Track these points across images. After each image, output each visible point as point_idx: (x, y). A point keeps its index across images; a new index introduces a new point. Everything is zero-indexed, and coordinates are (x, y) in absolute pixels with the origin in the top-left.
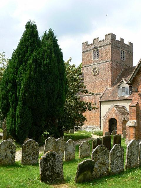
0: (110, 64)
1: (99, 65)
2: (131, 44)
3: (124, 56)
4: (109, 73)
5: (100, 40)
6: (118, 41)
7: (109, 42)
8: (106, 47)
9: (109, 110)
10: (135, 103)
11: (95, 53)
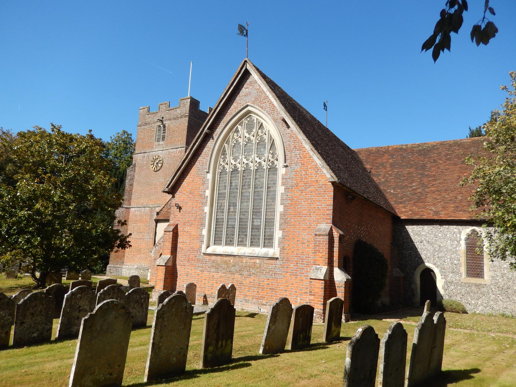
1: (163, 152)
7: (186, 113)
8: (180, 120)
11: (160, 130)
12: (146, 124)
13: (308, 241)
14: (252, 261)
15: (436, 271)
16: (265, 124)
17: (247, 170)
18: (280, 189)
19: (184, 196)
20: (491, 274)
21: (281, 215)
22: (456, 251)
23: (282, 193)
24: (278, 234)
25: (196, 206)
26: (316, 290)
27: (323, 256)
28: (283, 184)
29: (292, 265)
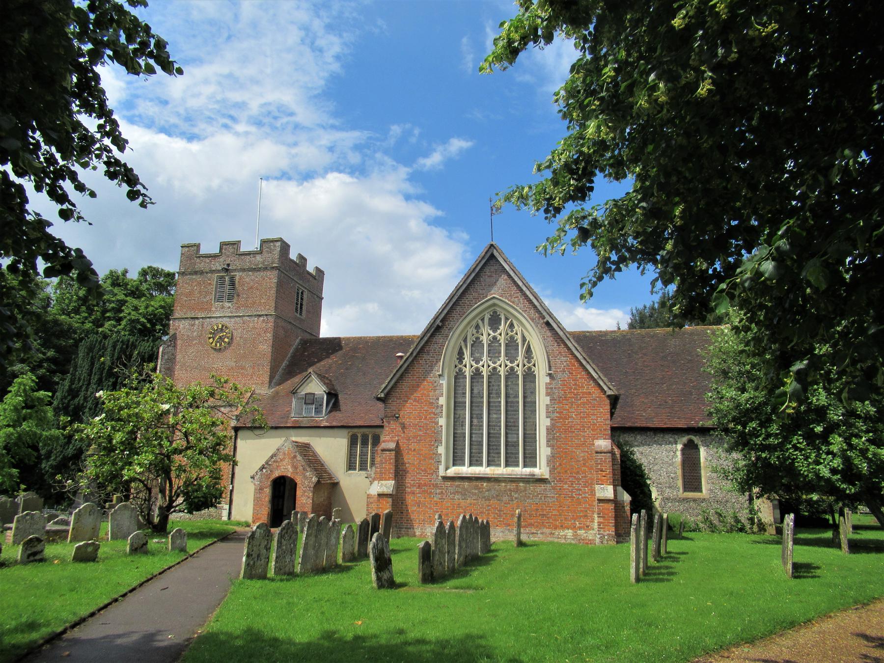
0: (271, 325)
1: (233, 320)
2: (320, 272)
3: (301, 305)
4: (265, 347)
5: (243, 249)
6: (292, 261)
10: (392, 441)
12: (196, 273)
16: (515, 323)
18: (542, 401)
20: (709, 486)
21: (547, 429)
24: (543, 451)
28: (548, 394)
29: (566, 486)
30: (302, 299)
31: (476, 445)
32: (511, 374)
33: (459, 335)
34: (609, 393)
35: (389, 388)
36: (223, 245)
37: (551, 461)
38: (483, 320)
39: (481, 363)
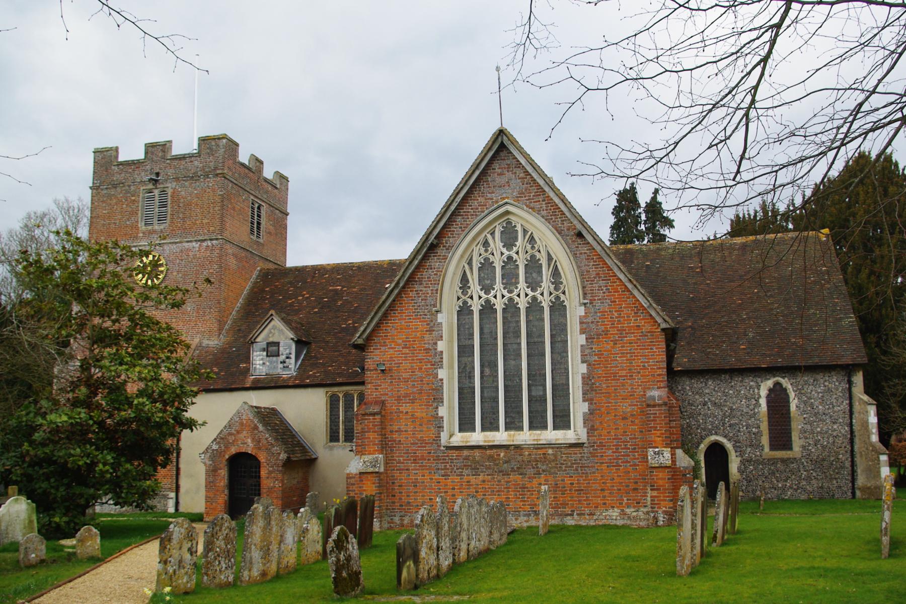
3: (259, 224)
5: (176, 151)
6: (243, 165)
7: (216, 168)
9: (230, 425)
13: (632, 415)
14: (540, 452)
15: (729, 445)
17: (511, 308)
18: (576, 340)
19: (391, 351)
20: (802, 442)
21: (583, 378)
22: (755, 414)
23: (582, 346)
24: (578, 408)
25: (420, 369)
26: (661, 482)
27: (662, 434)
28: (582, 331)
30: (259, 216)
31: (490, 402)
32: (534, 307)
33: (462, 256)
34: (664, 326)
35: (368, 331)
36: (150, 148)
37: (588, 419)
38: (493, 234)
39: (493, 292)
